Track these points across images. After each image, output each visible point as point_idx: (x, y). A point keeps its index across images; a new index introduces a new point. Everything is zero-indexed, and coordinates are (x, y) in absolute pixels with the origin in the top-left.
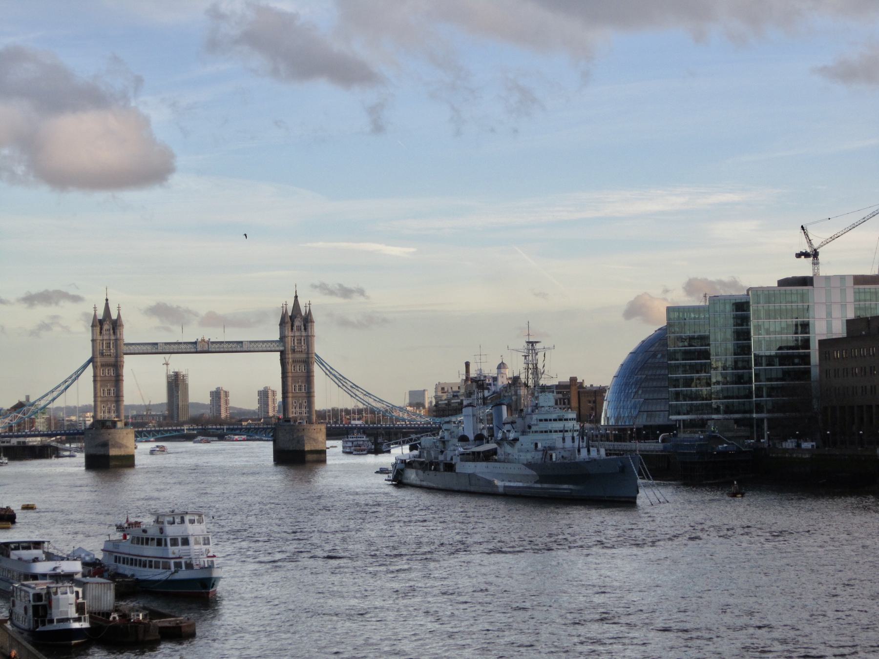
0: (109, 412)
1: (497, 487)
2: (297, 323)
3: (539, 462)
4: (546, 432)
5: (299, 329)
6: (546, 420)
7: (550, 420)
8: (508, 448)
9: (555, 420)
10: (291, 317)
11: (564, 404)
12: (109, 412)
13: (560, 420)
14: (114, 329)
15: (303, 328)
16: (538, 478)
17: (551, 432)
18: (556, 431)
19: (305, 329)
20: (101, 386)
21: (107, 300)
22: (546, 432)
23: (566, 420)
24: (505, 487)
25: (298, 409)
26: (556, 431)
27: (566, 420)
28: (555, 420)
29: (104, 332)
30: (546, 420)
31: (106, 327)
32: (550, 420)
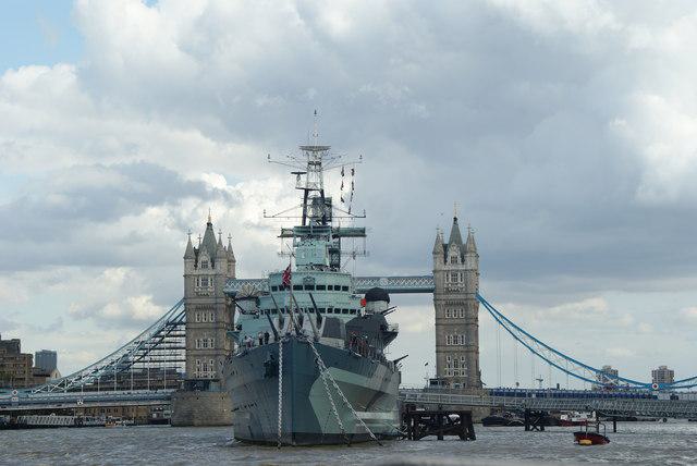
0: (205, 370)
2: (453, 252)
5: (454, 260)
10: (445, 247)
12: (205, 370)
13: (310, 287)
14: (213, 262)
15: (459, 259)
19: (463, 261)
20: (196, 335)
21: (209, 224)
23: (321, 288)
25: (453, 368)
27: (321, 288)
29: (199, 265)
31: (203, 258)
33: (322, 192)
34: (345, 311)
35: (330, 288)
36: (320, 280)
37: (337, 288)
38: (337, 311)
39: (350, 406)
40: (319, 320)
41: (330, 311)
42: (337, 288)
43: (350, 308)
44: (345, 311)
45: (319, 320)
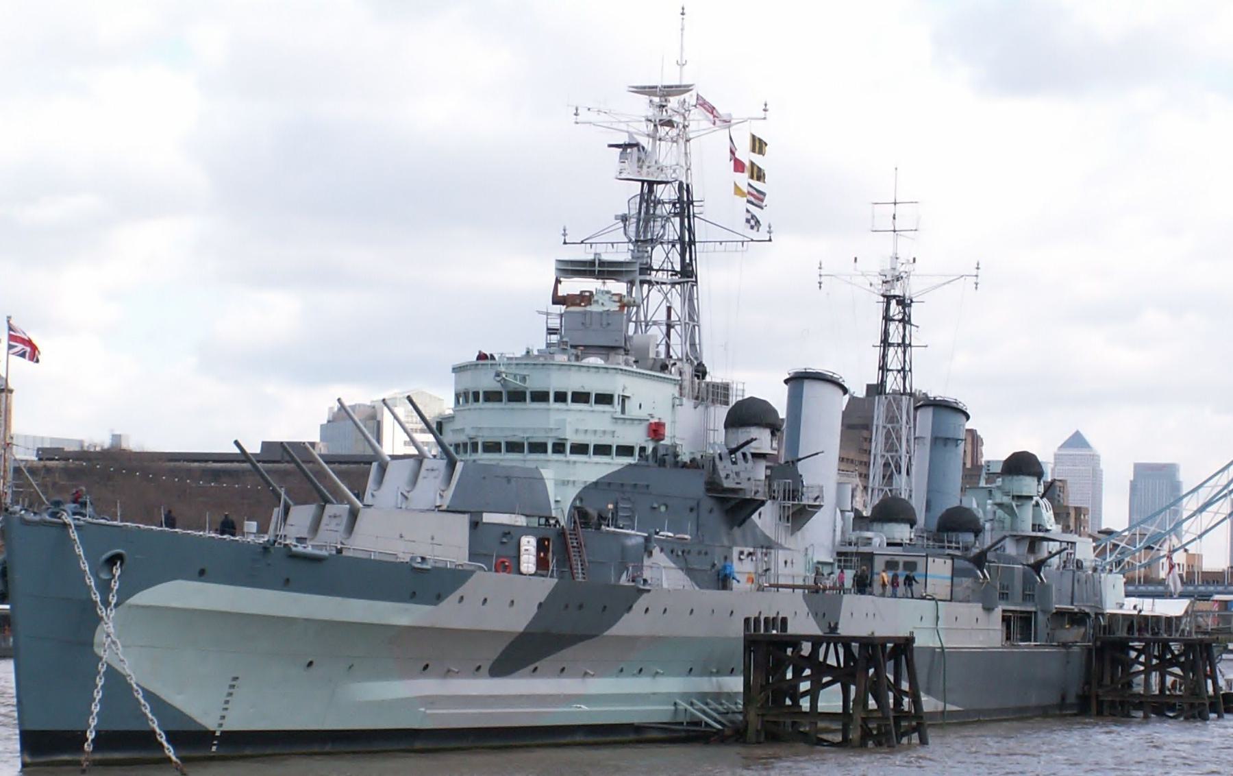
9: (492, 396)
13: (517, 396)
23: (540, 397)
27: (540, 397)
28: (492, 396)
33: (684, 189)
34: (602, 450)
35: (561, 397)
36: (536, 382)
37: (581, 397)
38: (580, 449)
39: (100, 682)
40: (452, 465)
41: (559, 448)
42: (581, 397)
43: (615, 442)
44: (602, 450)
45: (452, 465)
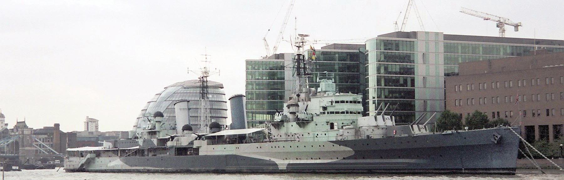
1: (276, 165)
3: (350, 138)
4: (343, 113)
6: (343, 102)
7: (347, 102)
8: (292, 128)
9: (351, 102)
11: (49, 141)
13: (355, 102)
16: (353, 153)
17: (347, 113)
18: (351, 113)
22: (343, 113)
24: (289, 164)
26: (351, 113)
28: (351, 102)
30: (343, 102)
32: (347, 102)
